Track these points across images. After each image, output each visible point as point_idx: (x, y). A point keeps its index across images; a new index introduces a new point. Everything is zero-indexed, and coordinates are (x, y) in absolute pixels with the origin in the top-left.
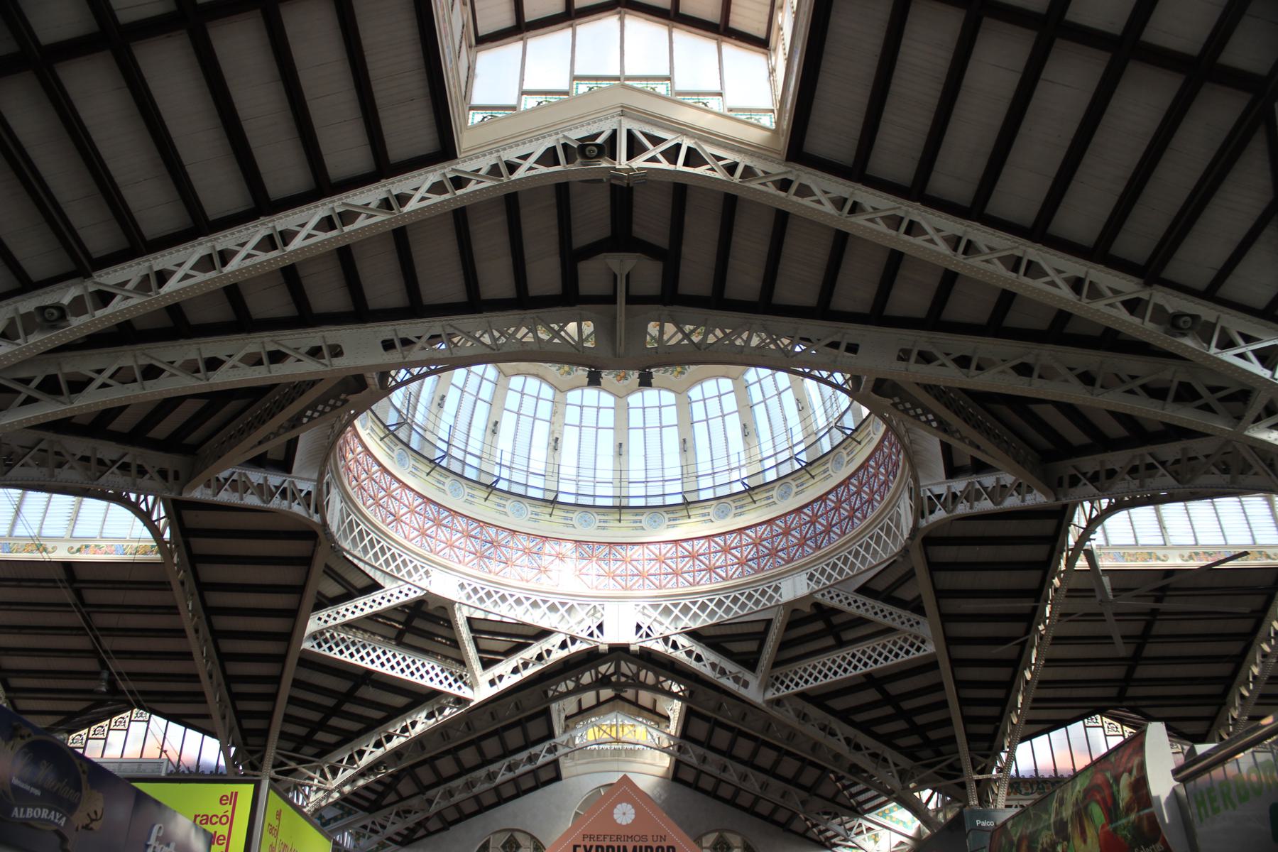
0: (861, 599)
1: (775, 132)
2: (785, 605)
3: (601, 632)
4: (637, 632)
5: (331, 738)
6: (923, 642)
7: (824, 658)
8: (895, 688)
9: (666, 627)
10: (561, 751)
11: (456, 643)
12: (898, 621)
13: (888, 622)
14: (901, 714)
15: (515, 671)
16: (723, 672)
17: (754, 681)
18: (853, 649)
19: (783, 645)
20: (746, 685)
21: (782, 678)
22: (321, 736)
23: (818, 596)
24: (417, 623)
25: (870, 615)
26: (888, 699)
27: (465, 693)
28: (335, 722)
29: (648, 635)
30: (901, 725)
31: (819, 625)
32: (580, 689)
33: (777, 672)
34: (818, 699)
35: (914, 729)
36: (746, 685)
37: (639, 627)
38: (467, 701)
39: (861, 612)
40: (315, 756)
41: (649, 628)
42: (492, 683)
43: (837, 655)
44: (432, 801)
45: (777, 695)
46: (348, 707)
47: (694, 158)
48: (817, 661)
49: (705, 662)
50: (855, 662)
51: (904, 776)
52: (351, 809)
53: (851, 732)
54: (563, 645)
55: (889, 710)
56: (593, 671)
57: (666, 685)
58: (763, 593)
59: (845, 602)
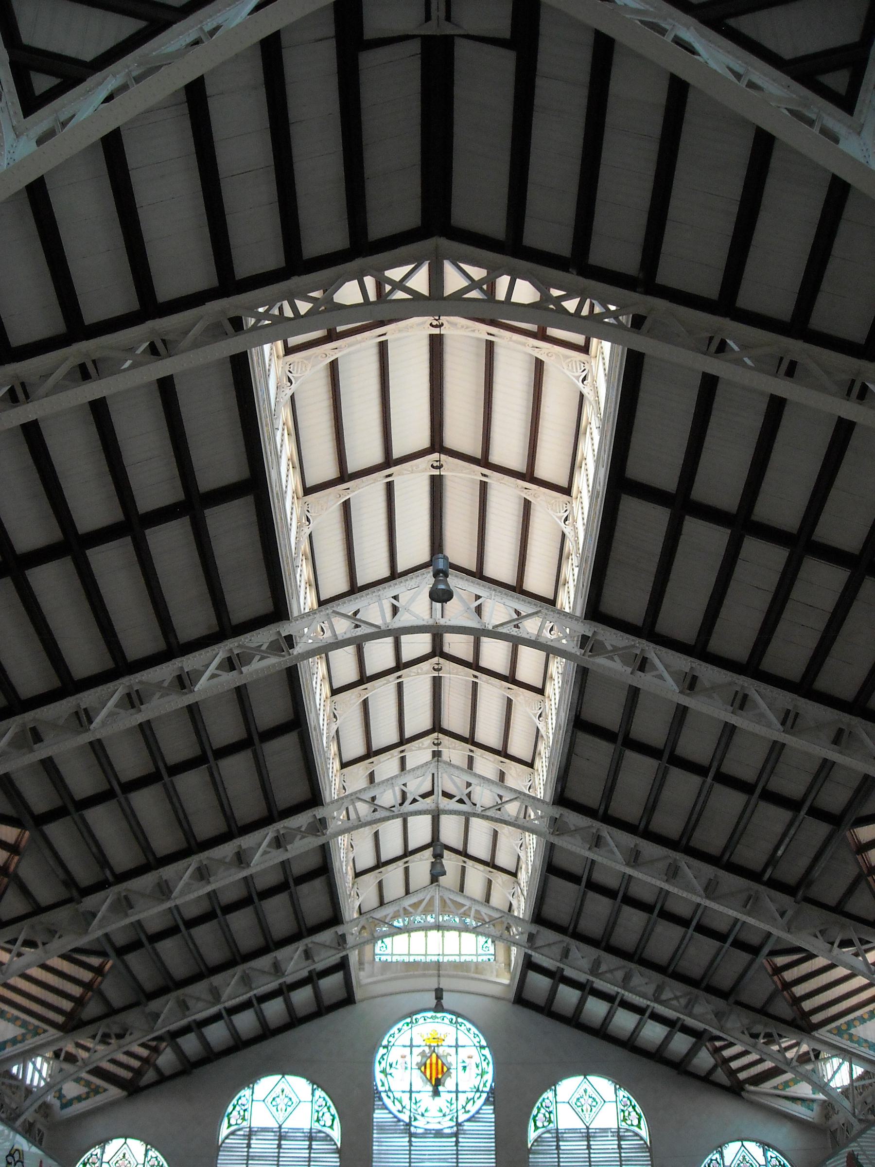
44: (94, 915)
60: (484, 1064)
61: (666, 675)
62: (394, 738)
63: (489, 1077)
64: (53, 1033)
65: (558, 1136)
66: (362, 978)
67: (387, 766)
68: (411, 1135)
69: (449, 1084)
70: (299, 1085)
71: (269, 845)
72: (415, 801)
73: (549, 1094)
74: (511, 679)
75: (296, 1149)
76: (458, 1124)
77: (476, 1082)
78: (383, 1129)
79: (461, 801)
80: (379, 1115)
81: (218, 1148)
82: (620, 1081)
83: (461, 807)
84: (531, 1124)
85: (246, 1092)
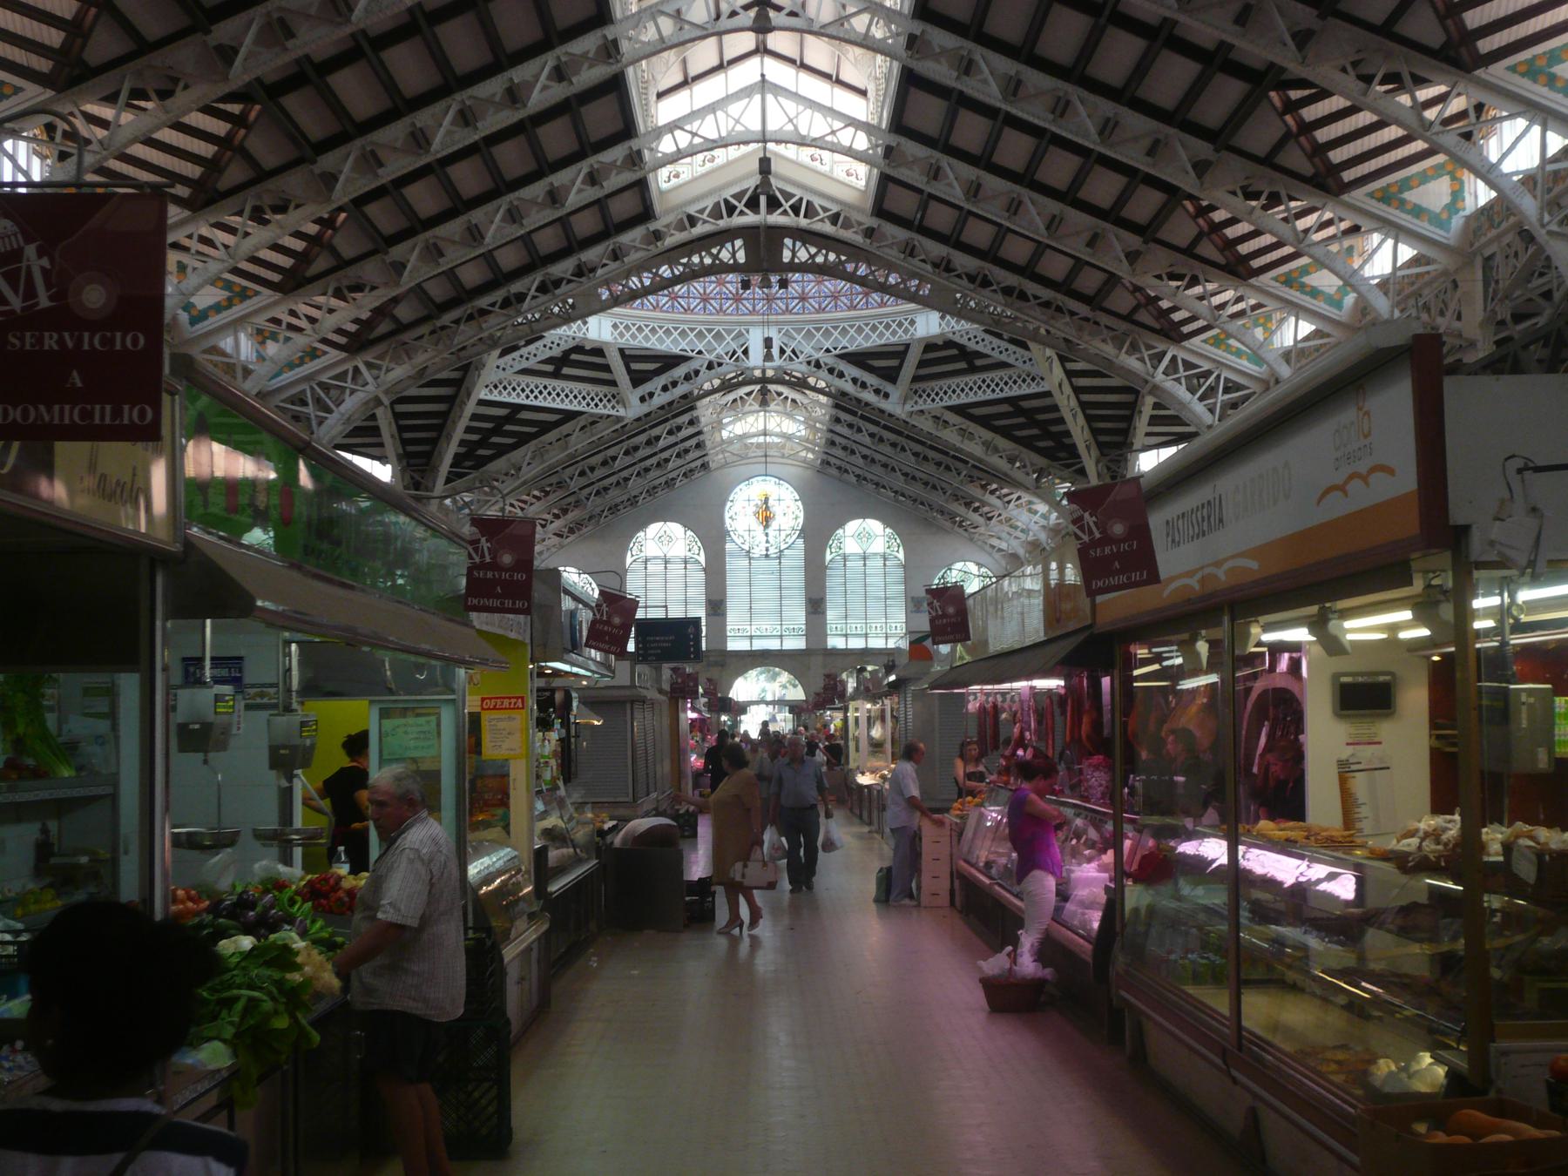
0: (988, 338)
1: (864, 192)
2: (921, 339)
6: (1042, 379)
7: (956, 380)
8: (1025, 404)
9: (808, 349)
11: (606, 368)
12: (1021, 360)
13: (1011, 360)
14: (1037, 424)
15: (665, 389)
16: (864, 385)
17: (896, 392)
18: (984, 376)
19: (922, 364)
20: (886, 396)
21: (920, 392)
22: (481, 452)
23: (951, 335)
24: (574, 357)
25: (995, 354)
26: (1020, 412)
27: (622, 412)
30: (1035, 431)
31: (954, 352)
33: (916, 386)
34: (960, 410)
35: (1048, 435)
36: (886, 396)
38: (619, 419)
39: (987, 351)
40: (469, 468)
41: (793, 351)
42: (642, 399)
43: (970, 379)
45: (916, 408)
46: (508, 427)
47: (811, 212)
48: (953, 382)
49: (848, 378)
50: (984, 387)
51: (1041, 473)
53: (987, 435)
55: (1021, 420)
58: (900, 325)
59: (973, 341)
60: (797, 512)
61: (955, 184)
63: (801, 520)
65: (845, 558)
66: (715, 459)
68: (750, 559)
69: (774, 525)
70: (675, 528)
71: (549, 78)
72: (733, 14)
73: (840, 531)
75: (676, 570)
76: (781, 551)
77: (792, 523)
78: (732, 555)
79: (793, 14)
80: (729, 546)
81: (626, 571)
82: (887, 523)
83: (793, 21)
84: (828, 551)
85: (641, 534)
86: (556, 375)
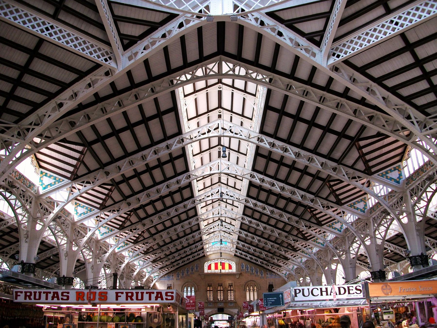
3: (208, 10)
4: (234, 11)
5: (23, 108)
10: (186, 141)
28: (21, 92)
29: (243, 10)
32: (195, 79)
37: (236, 7)
52: (60, 179)
54: (181, 25)
56: (204, 68)
57: (254, 75)
62: (206, 110)
64: (96, 210)
67: (203, 120)
74: (245, 91)
86: (55, 17)
